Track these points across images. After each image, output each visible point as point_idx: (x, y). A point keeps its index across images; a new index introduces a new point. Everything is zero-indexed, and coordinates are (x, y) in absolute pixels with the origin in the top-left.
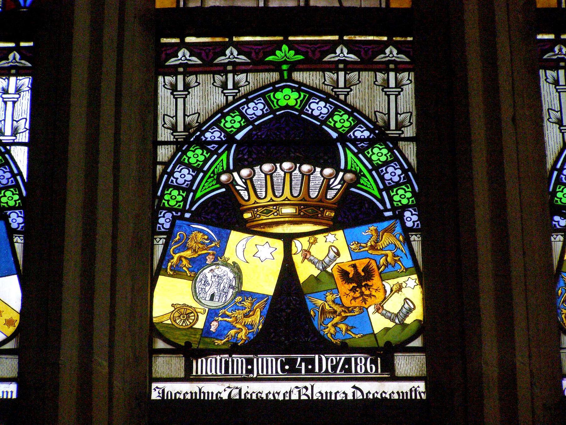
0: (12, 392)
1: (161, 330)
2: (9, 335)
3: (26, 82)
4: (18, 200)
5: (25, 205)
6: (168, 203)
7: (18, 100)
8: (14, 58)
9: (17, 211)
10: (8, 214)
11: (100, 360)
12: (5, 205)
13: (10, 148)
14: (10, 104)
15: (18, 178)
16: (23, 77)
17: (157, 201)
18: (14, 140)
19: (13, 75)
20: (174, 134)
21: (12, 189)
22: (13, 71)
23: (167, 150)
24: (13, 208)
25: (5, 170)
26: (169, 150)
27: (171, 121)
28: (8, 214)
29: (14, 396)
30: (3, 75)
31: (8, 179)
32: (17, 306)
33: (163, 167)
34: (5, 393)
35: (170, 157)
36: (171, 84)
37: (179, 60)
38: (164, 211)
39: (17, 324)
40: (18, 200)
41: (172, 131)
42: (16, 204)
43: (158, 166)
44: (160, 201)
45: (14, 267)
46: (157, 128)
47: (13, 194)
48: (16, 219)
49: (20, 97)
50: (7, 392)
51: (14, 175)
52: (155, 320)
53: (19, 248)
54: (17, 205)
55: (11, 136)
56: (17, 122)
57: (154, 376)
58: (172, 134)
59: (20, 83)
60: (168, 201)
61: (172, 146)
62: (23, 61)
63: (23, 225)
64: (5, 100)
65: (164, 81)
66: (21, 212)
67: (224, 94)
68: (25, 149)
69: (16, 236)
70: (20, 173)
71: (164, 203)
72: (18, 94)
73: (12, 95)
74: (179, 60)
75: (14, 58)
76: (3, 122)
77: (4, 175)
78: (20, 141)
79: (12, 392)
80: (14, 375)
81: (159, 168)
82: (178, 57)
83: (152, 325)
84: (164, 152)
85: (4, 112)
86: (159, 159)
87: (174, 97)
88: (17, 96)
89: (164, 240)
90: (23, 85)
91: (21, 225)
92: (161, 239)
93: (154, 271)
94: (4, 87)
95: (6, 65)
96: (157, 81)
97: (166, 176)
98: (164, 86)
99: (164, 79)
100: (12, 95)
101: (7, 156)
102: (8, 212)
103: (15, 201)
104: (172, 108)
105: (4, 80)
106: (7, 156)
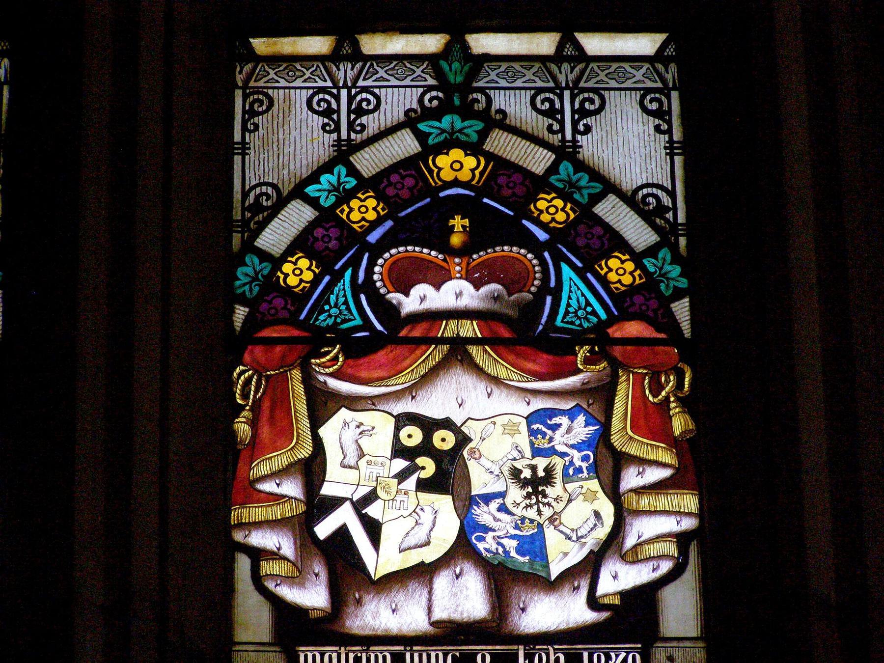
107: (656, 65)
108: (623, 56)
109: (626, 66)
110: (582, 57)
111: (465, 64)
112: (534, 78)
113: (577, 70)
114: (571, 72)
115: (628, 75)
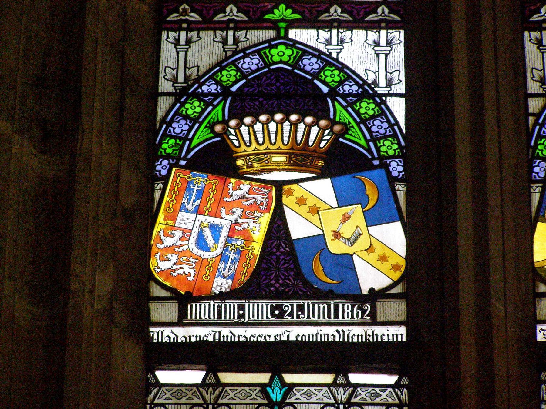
0: (402, 335)
1: (543, 274)
2: (395, 280)
3: (398, 35)
4: (397, 149)
5: (404, 155)
6: (542, 153)
7: (390, 53)
8: (383, 12)
9: (397, 160)
10: (388, 162)
11: (498, 305)
12: (385, 154)
13: (386, 99)
14: (382, 57)
15: (396, 127)
16: (394, 31)
17: (531, 150)
18: (389, 91)
19: (383, 28)
20: (543, 86)
21: (390, 139)
22: (383, 25)
23: (537, 102)
24: (393, 157)
25: (382, 120)
26: (540, 102)
27: (539, 75)
28: (388, 162)
29: (404, 339)
30: (374, 28)
31: (386, 129)
32: (403, 251)
33: (535, 118)
34: (395, 337)
35: (541, 109)
36: (537, 39)
37: (542, 16)
38: (539, 161)
39: (403, 269)
40: (397, 149)
41: (541, 84)
42: (395, 153)
43: (530, 117)
44: (534, 152)
45: (396, 213)
46: (526, 82)
47: (392, 144)
48: (396, 168)
49: (391, 50)
50: (397, 335)
51: (391, 126)
52: (536, 265)
53: (401, 195)
54: (397, 154)
55: (386, 87)
56: (391, 73)
57: (538, 318)
58: (541, 86)
59: (390, 36)
60: (542, 151)
61: (542, 98)
62: (392, 15)
63: (403, 173)
64: (377, 52)
65: (530, 36)
66: (400, 161)
67: (540, 50)
68: (403, 100)
69: (397, 184)
70: (397, 123)
71: (538, 153)
72: (390, 46)
73: (383, 47)
74: (542, 16)
75: (383, 12)
76: (377, 74)
77: (381, 124)
78: (395, 92)
79: (402, 335)
80: (403, 319)
81: (531, 119)
82: (541, 13)
83: (534, 270)
84: (534, 104)
85: (377, 64)
86: (531, 110)
87: (540, 52)
88: (389, 49)
89: (541, 188)
90: (394, 38)
91: (401, 174)
92: (537, 187)
93: (533, 218)
94: (376, 39)
95: (376, 18)
96: (523, 36)
97: (538, 127)
98: (530, 40)
99: (530, 34)
100: (383, 47)
101: (383, 106)
102: (389, 161)
103: (395, 150)
104: (539, 62)
105: (375, 32)
106: (383, 106)
107: (332, 388)
108: (365, 384)
109: (247, 389)
110: (219, 384)
111: (283, 388)
112: (322, 397)
113: (217, 392)
114: (344, 394)
115: (183, 394)
